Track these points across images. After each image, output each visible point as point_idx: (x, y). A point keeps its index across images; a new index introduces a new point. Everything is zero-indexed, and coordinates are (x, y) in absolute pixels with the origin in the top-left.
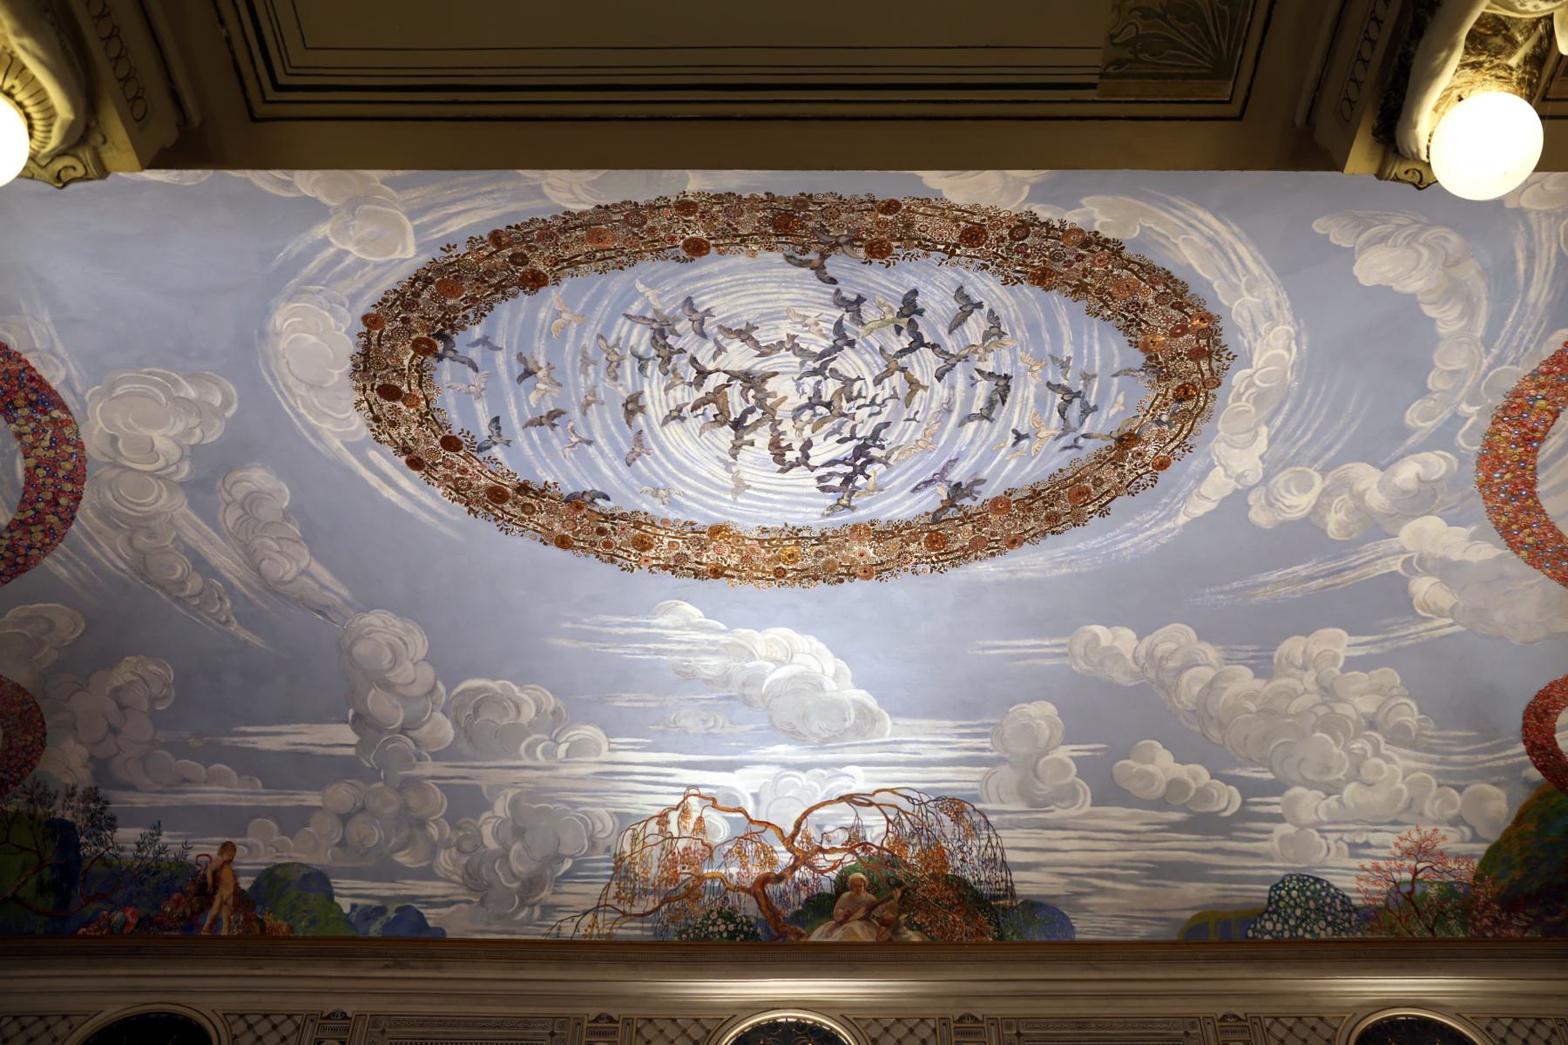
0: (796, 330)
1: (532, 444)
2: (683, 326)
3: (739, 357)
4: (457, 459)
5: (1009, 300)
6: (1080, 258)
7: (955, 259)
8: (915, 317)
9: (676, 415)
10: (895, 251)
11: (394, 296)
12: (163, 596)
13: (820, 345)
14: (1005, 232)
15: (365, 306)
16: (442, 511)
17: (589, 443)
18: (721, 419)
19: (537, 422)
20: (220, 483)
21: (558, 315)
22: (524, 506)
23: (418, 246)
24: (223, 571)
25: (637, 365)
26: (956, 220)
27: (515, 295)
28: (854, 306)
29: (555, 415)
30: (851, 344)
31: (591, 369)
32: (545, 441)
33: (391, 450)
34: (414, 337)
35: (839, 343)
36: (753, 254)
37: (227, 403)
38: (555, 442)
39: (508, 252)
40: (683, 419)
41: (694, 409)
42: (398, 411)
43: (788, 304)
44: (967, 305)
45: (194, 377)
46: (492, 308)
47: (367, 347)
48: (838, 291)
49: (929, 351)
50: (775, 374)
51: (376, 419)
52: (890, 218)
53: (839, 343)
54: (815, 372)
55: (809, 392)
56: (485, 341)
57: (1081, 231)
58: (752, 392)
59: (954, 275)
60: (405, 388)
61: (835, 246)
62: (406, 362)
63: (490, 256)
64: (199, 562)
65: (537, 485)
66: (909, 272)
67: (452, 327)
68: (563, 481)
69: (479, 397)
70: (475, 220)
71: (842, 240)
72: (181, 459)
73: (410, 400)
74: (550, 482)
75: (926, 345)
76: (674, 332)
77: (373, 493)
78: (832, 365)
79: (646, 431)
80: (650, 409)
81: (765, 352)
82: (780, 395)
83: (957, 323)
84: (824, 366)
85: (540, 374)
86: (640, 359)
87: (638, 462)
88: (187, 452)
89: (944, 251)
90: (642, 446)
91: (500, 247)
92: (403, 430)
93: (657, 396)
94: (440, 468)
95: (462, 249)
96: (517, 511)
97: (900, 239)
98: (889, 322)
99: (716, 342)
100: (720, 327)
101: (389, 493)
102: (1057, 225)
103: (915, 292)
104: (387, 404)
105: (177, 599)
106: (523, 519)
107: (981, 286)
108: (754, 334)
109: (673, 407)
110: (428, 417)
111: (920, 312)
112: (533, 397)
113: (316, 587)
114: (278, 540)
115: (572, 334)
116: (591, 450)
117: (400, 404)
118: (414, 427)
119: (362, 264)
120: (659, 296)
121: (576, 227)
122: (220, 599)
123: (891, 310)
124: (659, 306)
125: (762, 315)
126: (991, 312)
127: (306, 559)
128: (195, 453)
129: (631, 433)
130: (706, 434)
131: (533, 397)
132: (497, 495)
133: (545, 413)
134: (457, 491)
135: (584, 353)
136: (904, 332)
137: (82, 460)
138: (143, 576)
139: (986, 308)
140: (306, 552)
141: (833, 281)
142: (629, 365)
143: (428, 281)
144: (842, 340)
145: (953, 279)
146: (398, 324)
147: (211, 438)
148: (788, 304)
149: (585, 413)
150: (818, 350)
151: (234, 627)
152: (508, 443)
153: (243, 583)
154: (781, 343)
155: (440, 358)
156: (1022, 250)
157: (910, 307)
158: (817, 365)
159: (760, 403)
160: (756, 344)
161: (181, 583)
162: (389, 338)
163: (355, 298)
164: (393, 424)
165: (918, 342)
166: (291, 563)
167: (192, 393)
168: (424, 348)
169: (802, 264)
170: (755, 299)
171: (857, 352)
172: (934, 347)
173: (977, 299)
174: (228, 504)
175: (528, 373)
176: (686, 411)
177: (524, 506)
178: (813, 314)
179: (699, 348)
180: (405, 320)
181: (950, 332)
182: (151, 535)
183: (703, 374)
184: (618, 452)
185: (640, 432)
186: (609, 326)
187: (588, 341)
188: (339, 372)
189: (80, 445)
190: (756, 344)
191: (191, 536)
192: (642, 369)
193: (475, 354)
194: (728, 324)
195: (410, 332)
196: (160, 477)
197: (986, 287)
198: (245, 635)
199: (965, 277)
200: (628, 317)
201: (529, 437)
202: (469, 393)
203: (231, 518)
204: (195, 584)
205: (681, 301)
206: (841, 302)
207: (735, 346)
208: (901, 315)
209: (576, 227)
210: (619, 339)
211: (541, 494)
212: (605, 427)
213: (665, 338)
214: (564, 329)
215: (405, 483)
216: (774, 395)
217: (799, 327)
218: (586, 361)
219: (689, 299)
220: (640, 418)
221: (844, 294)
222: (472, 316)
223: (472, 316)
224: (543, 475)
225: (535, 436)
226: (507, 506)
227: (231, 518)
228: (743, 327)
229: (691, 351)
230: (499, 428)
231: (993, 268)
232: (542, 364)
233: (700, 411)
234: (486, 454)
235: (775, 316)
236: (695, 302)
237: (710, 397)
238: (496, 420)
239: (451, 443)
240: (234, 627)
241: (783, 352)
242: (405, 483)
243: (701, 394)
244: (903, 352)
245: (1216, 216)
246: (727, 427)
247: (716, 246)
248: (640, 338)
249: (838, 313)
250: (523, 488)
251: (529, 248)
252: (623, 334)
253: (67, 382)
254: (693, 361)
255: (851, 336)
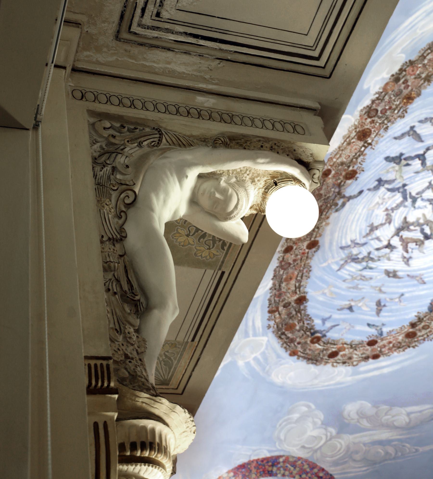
0: (383, 208)
1: (389, 316)
2: (355, 251)
3: (386, 233)
4: (380, 343)
5: (417, 113)
6: (406, 82)
7: (373, 143)
8: (403, 157)
9: (407, 261)
10: (355, 168)
11: (285, 345)
12: (389, 462)
13: (398, 197)
14: (369, 120)
15: (285, 354)
16: (407, 357)
17: (402, 295)
18: (419, 243)
19: (379, 312)
20: (346, 421)
21: (324, 294)
22: (424, 328)
23: (263, 335)
24: (390, 438)
25: (368, 270)
26: (349, 144)
27: (305, 307)
28: (380, 182)
29: (379, 303)
30: (404, 185)
31: (360, 286)
32: (391, 311)
33: (363, 363)
34: (309, 342)
35: (401, 190)
36: (327, 224)
37: (308, 407)
38: (394, 307)
39: (281, 308)
40: (410, 258)
41: (407, 251)
42: (344, 355)
43: (365, 210)
44: (412, 132)
45: (290, 412)
46: (308, 315)
47: (304, 358)
48: (369, 190)
49: (429, 152)
50: (405, 218)
51: (344, 363)
52: (333, 172)
53: (401, 190)
54: (414, 200)
55: (427, 203)
56: (324, 320)
57: (387, 84)
58: (412, 227)
59: (384, 142)
60: (334, 350)
61: (339, 193)
62: (320, 347)
63: (280, 314)
64: (381, 443)
65: (415, 320)
66: (372, 161)
67: (310, 329)
68: (420, 310)
69: (353, 327)
70: (259, 318)
71: (337, 190)
72: (326, 429)
73: (340, 350)
74: (416, 314)
75: (425, 153)
76: (356, 255)
77: (382, 376)
78: (414, 194)
79: (409, 273)
80: (396, 268)
81: (389, 220)
82: (421, 216)
83: (419, 138)
84: (411, 197)
85: (353, 304)
86: (365, 268)
87: (426, 280)
88: (324, 426)
89: (366, 147)
90: (416, 277)
91: (277, 310)
92: (355, 356)
93: (395, 262)
94: (383, 350)
95: (272, 323)
96: (424, 332)
97: (349, 167)
98: (400, 169)
99: (372, 239)
100: (364, 237)
101: (385, 371)
102: (377, 96)
103: (388, 159)
104: (339, 357)
105: (394, 458)
106: (430, 331)
107: (399, 129)
108: (375, 224)
109: (401, 260)
110: (353, 346)
111: (402, 154)
112: (364, 308)
113: (419, 414)
114: (386, 414)
115: (336, 290)
116: (407, 295)
117: (341, 353)
118: (355, 352)
119: (263, 354)
120: (333, 258)
121: (280, 286)
122: (404, 446)
123: (393, 167)
124: (339, 259)
125: (366, 220)
126: (421, 122)
127: (404, 411)
128: (325, 424)
129: (407, 278)
130: (425, 251)
131: (364, 308)
132: (411, 336)
133: (376, 307)
134: (399, 348)
135: (350, 288)
136: (410, 162)
137: (306, 461)
138: (375, 463)
139: (417, 124)
140: (398, 409)
141: (361, 192)
142: (366, 273)
143: (283, 334)
144: (403, 189)
145: (387, 142)
146: (299, 346)
147: (322, 417)
148: (365, 210)
149: (384, 293)
150: (401, 199)
151: (421, 449)
152: (383, 325)
153: (400, 435)
154: (387, 215)
155: (325, 336)
156: (384, 111)
157: (397, 160)
158: (410, 200)
159: (419, 225)
160: (382, 225)
161: (387, 453)
162: (305, 350)
163: (278, 356)
164: (350, 358)
165: (422, 157)
166: (401, 416)
167: (296, 416)
168: (317, 340)
169: (344, 205)
170: (354, 224)
171: (412, 183)
172: (428, 149)
173: (408, 129)
174: (358, 422)
175: (350, 308)
176: (406, 255)
177: (424, 328)
178: (377, 199)
179: (371, 246)
180: (299, 343)
181: (422, 141)
182: (357, 452)
183: (389, 246)
184: (414, 286)
185: (408, 276)
186: (340, 277)
187: (344, 285)
188: (313, 368)
189: (299, 459)
190: (382, 225)
191: (366, 439)
192: (371, 268)
193: (328, 324)
194: (364, 234)
195: (306, 343)
196: (330, 439)
197: (400, 126)
198: (427, 448)
199: (389, 137)
200: (339, 270)
201: (385, 316)
202: (349, 329)
203: (365, 423)
204: (391, 450)
205: (341, 251)
206: (376, 188)
207: (378, 233)
208: (398, 163)
209: (280, 286)
210: (349, 275)
211: (420, 320)
212: (398, 287)
213: (358, 258)
214: (332, 293)
215: (384, 364)
216: (418, 219)
217: (382, 206)
218: (356, 287)
219: (342, 248)
220: (400, 274)
221: (372, 187)
222: (308, 322)
223: (308, 322)
224: (412, 316)
225: (386, 314)
226: (419, 334)
227: (365, 423)
228: (369, 229)
229: (371, 249)
230: (373, 325)
231: (389, 124)
232: (347, 303)
233: (410, 250)
234: (385, 335)
235: (370, 215)
236: (344, 244)
237: (404, 244)
238: (369, 325)
239: (372, 343)
240: (421, 449)
241: (393, 215)
242: (384, 364)
243: (400, 248)
244: (423, 163)
245: (411, 16)
246: (427, 242)
247: (316, 237)
248: (353, 267)
249: (382, 189)
250: (413, 325)
251: (283, 301)
252: (347, 273)
253: (269, 451)
254: (378, 249)
255: (400, 185)
